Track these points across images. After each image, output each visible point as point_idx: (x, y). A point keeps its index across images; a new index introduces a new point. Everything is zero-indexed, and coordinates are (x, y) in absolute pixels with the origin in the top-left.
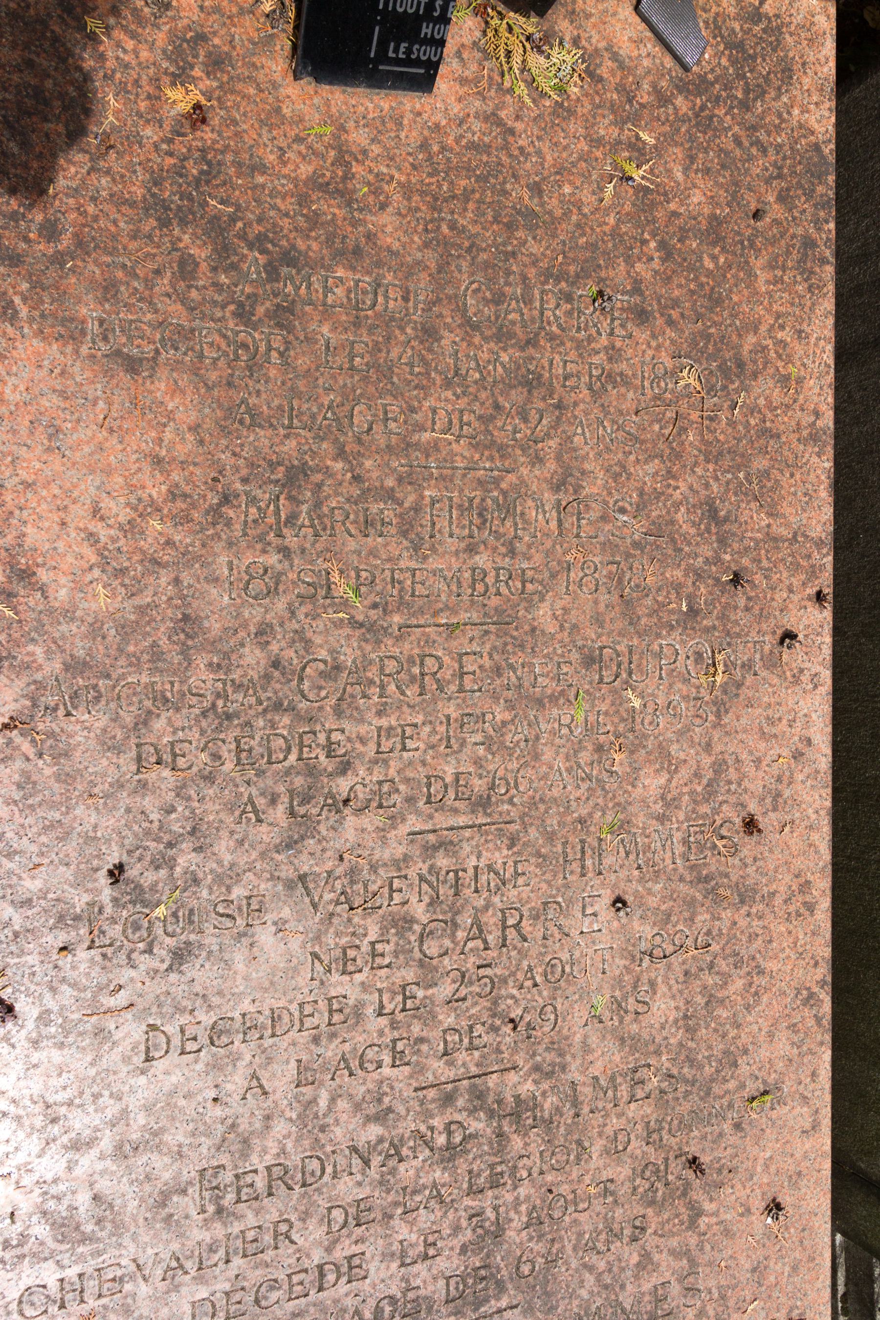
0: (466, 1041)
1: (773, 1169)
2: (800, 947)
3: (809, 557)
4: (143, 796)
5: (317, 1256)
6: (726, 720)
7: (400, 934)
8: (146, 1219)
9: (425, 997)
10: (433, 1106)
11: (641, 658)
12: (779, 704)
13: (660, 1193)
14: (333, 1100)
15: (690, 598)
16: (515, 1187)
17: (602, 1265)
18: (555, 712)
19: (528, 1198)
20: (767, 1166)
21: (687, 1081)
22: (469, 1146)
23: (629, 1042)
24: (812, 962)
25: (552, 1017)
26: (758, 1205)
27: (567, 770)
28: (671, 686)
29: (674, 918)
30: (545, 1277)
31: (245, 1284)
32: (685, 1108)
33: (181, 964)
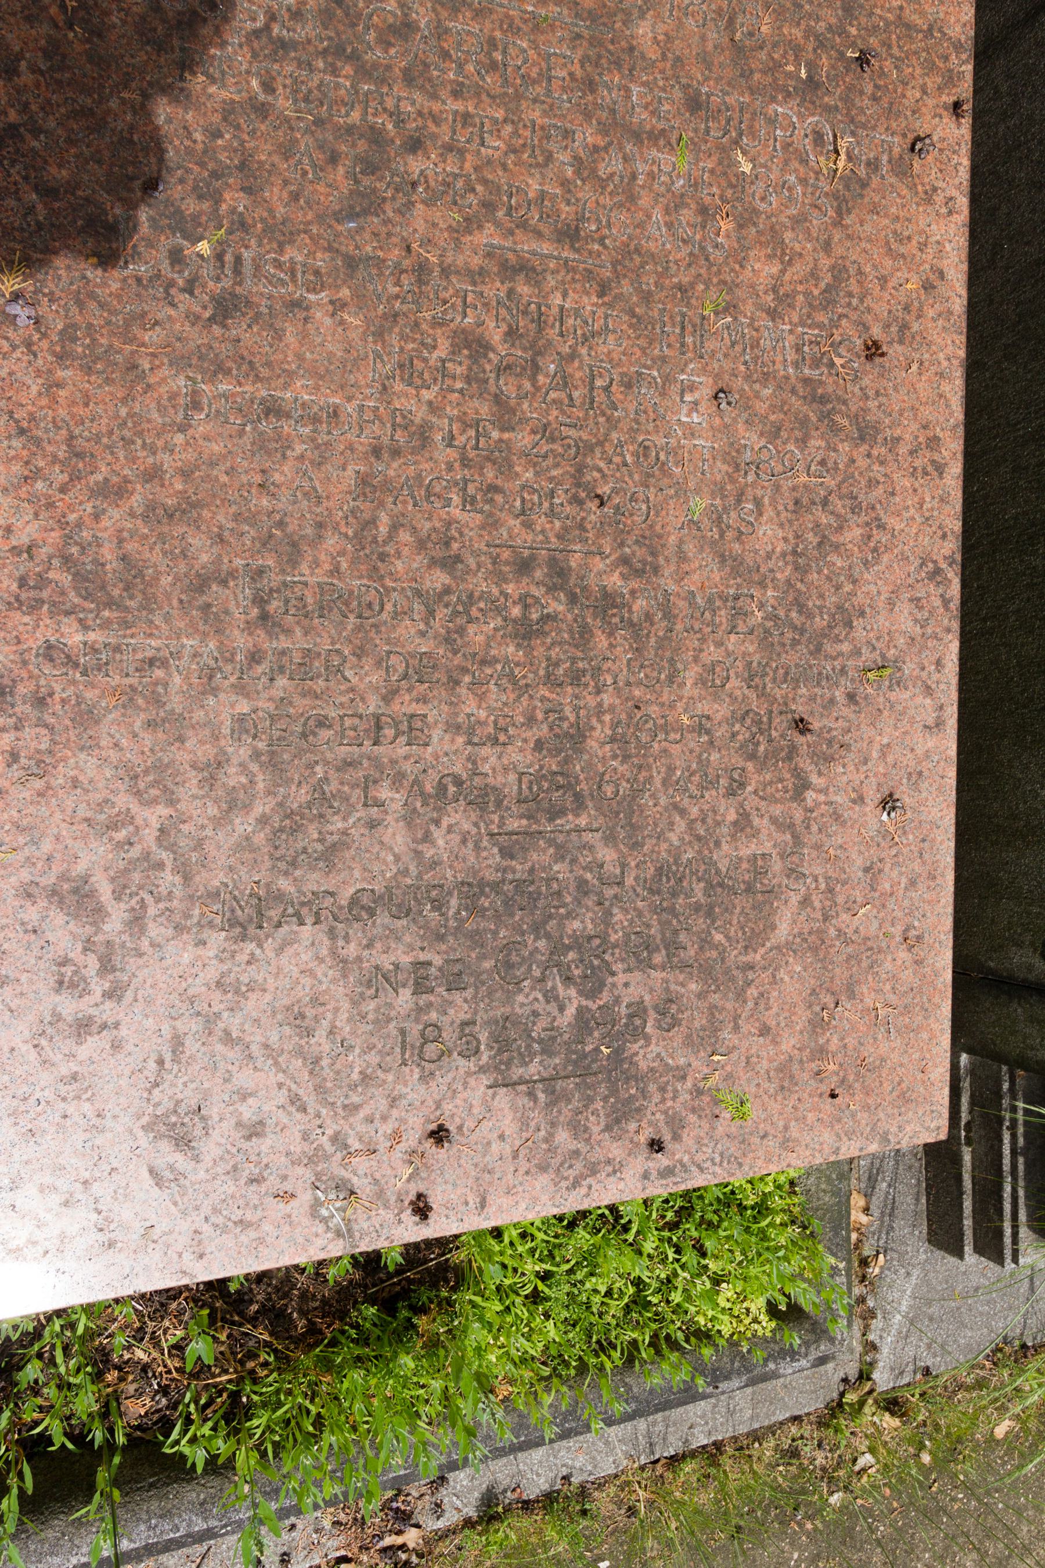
0: (546, 505)
1: (890, 759)
2: (926, 513)
3: (946, 58)
4: (186, 110)
5: (373, 705)
6: (848, 221)
7: (474, 358)
8: (181, 601)
9: (501, 440)
10: (507, 569)
11: (752, 119)
12: (909, 220)
13: (762, 748)
14: (394, 528)
15: (811, 66)
16: (598, 692)
17: (694, 811)
18: (654, 152)
19: (612, 709)
20: (883, 755)
21: (795, 628)
22: (547, 628)
23: (729, 562)
24: (940, 533)
25: (644, 507)
26: (873, 797)
27: (666, 224)
28: (786, 162)
29: (784, 434)
30: (630, 806)
31: (291, 710)
32: (790, 658)
33: (225, 318)
